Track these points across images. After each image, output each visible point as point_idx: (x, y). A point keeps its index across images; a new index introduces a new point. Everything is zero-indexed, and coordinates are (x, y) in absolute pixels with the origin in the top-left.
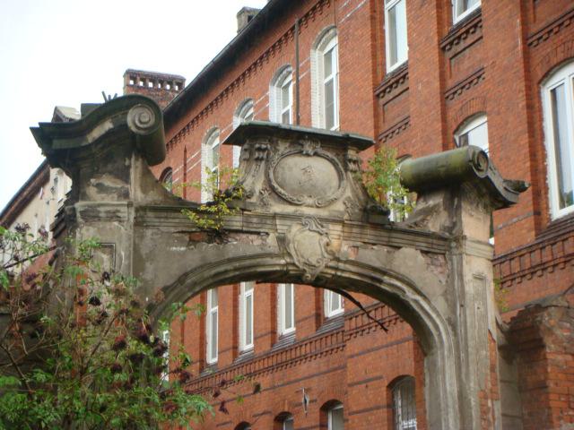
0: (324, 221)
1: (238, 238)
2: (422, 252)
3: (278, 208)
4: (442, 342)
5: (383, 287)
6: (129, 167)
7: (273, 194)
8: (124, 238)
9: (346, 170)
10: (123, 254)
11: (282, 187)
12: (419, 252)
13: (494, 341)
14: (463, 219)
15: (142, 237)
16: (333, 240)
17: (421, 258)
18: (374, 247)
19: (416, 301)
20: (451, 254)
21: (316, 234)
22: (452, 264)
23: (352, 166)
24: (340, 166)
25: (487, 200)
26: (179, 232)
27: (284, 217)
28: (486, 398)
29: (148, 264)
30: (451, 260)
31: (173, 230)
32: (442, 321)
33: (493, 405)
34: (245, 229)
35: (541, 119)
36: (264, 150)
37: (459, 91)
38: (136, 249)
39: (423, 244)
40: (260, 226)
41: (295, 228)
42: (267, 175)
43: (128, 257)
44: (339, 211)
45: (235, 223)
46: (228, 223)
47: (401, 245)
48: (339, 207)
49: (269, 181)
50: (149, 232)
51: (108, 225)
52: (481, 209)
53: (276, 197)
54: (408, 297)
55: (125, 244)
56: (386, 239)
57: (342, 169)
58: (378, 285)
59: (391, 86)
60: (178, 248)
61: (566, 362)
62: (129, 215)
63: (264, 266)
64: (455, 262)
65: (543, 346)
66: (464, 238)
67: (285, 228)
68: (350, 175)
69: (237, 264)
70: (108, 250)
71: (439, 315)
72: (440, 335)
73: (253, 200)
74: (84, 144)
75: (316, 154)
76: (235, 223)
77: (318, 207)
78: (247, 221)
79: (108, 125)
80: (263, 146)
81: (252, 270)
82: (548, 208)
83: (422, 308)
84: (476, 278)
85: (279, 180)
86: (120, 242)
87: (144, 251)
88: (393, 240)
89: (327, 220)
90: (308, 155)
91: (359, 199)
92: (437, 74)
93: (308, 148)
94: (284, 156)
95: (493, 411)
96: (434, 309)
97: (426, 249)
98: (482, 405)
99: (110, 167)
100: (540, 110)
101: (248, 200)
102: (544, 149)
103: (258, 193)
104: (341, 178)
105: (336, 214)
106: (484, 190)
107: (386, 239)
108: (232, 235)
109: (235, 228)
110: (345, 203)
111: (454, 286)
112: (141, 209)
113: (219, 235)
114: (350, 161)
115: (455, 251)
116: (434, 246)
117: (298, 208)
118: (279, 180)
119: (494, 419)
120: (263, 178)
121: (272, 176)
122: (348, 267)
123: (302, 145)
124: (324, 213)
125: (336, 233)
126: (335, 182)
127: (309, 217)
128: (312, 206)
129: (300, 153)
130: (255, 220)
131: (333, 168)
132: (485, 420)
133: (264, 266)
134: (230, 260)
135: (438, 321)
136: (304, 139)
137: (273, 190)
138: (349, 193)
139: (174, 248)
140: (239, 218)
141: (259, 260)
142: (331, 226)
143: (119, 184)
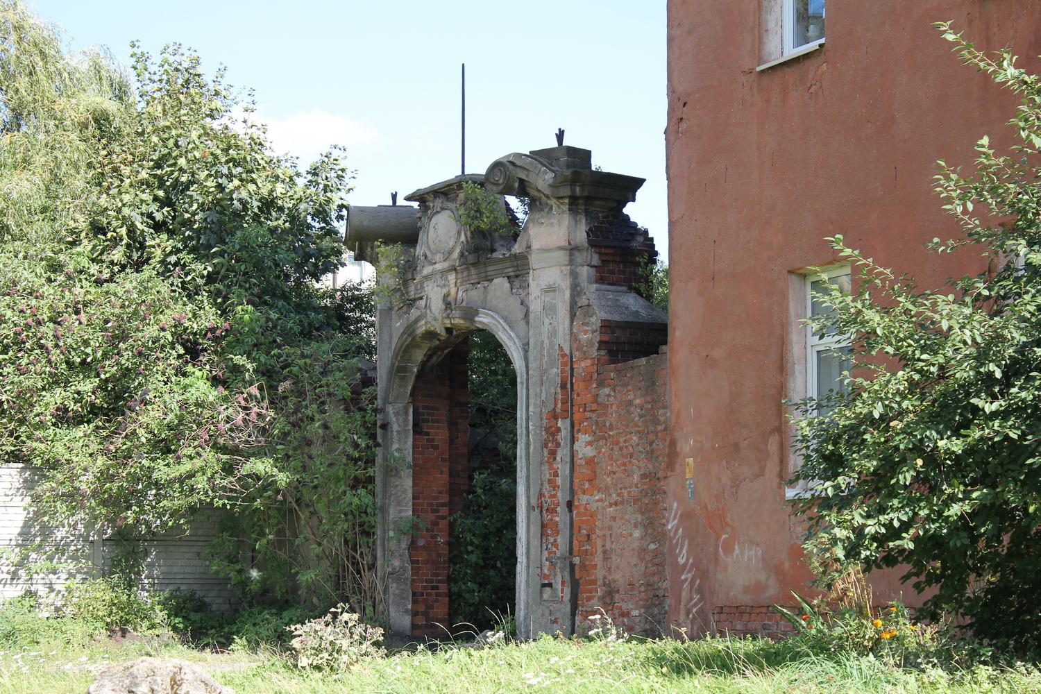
28: (556, 418)
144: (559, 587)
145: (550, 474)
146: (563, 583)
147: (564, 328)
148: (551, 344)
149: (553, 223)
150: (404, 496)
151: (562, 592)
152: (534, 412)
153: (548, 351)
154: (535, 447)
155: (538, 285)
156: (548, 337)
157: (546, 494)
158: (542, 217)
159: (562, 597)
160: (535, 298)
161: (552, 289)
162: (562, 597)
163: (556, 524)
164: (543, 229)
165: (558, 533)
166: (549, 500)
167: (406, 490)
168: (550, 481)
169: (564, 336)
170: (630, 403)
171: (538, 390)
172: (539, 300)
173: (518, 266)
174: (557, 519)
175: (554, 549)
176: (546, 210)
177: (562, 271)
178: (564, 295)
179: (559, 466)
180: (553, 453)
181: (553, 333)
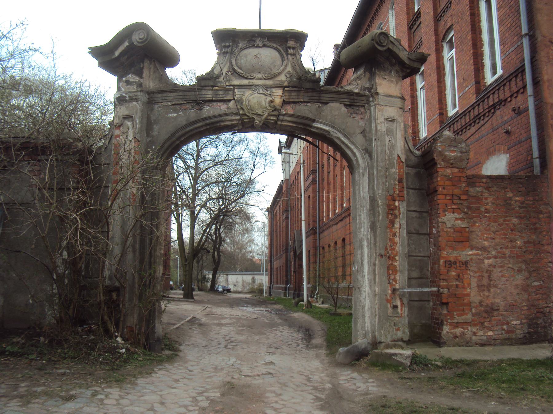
0: (267, 87)
1: (211, 105)
2: (346, 105)
3: (236, 82)
4: (358, 164)
5: (312, 130)
6: (143, 68)
7: (235, 74)
8: (139, 111)
9: (287, 54)
10: (138, 121)
11: (240, 68)
12: (343, 105)
13: (403, 163)
14: (377, 81)
15: (152, 110)
16: (276, 99)
17: (344, 109)
18: (308, 104)
19: (338, 138)
20: (370, 106)
21: (263, 96)
22: (370, 113)
23: (290, 51)
24: (282, 51)
25: (397, 67)
26: (172, 105)
27: (240, 86)
28: (394, 200)
29: (155, 126)
30: (370, 110)
31: (169, 104)
32: (359, 151)
33: (399, 205)
34: (214, 99)
35: (480, 21)
36: (229, 46)
37: (443, 15)
38: (148, 118)
39: (346, 100)
40: (224, 96)
41: (248, 93)
42: (230, 62)
43: (141, 122)
44: (281, 81)
45: (208, 96)
46: (205, 96)
47: (328, 101)
48: (283, 78)
49: (232, 65)
50: (156, 106)
51: (131, 105)
52: (393, 74)
53: (237, 75)
55: (139, 114)
56: (318, 98)
57: (284, 54)
58: (309, 129)
59: (415, 21)
60: (173, 115)
61: (453, 173)
62: (144, 98)
63: (226, 121)
64: (372, 111)
65: (435, 164)
66: (377, 94)
67: (242, 93)
68: (290, 57)
69: (208, 122)
70: (131, 119)
71: (356, 147)
72: (357, 160)
73: (221, 79)
74: (114, 57)
75: (264, 46)
76: (208, 96)
77: (265, 79)
78: (216, 93)
79: (126, 44)
80: (227, 44)
81: (218, 124)
82: (484, 78)
83: (343, 143)
84: (387, 120)
85: (239, 64)
86: (137, 113)
87: (153, 118)
88: (322, 98)
89: (271, 87)
90: (258, 47)
91: (297, 73)
92: (431, 6)
93: (259, 42)
94: (242, 49)
95: (399, 208)
96: (353, 143)
97: (348, 103)
98: (389, 206)
99: (133, 69)
100: (479, 15)
101: (217, 80)
102: (481, 40)
103: (224, 74)
104: (283, 61)
105: (278, 82)
106: (394, 61)
107: (318, 98)
108: (207, 104)
109: (207, 99)
110: (286, 75)
111: (371, 126)
112: (150, 93)
113: (199, 103)
114: (290, 48)
115: (372, 104)
116: (355, 101)
117: (250, 81)
118: (239, 64)
120: (228, 64)
121: (233, 62)
122: (287, 118)
123: (254, 41)
124: (269, 82)
125: (277, 94)
126: (279, 62)
127: (258, 86)
128: (261, 79)
129: (253, 46)
130: (221, 92)
131: (277, 54)
132: (392, 214)
133: (226, 121)
134: (204, 119)
135: (355, 151)
136: (256, 37)
137: (234, 70)
138: (289, 69)
139: (170, 115)
140: (210, 92)
141: (223, 118)
142: (274, 91)
143: (137, 79)
147: (401, 145)
148: (391, 153)
149: (392, 81)
152: (382, 194)
154: (383, 217)
158: (385, 75)
160: (381, 122)
161: (391, 120)
164: (384, 82)
169: (401, 150)
170: (510, 199)
171: (384, 180)
173: (354, 99)
174: (396, 264)
176: (388, 72)
177: (398, 111)
178: (400, 125)
179: (398, 230)
180: (392, 223)
181: (392, 147)
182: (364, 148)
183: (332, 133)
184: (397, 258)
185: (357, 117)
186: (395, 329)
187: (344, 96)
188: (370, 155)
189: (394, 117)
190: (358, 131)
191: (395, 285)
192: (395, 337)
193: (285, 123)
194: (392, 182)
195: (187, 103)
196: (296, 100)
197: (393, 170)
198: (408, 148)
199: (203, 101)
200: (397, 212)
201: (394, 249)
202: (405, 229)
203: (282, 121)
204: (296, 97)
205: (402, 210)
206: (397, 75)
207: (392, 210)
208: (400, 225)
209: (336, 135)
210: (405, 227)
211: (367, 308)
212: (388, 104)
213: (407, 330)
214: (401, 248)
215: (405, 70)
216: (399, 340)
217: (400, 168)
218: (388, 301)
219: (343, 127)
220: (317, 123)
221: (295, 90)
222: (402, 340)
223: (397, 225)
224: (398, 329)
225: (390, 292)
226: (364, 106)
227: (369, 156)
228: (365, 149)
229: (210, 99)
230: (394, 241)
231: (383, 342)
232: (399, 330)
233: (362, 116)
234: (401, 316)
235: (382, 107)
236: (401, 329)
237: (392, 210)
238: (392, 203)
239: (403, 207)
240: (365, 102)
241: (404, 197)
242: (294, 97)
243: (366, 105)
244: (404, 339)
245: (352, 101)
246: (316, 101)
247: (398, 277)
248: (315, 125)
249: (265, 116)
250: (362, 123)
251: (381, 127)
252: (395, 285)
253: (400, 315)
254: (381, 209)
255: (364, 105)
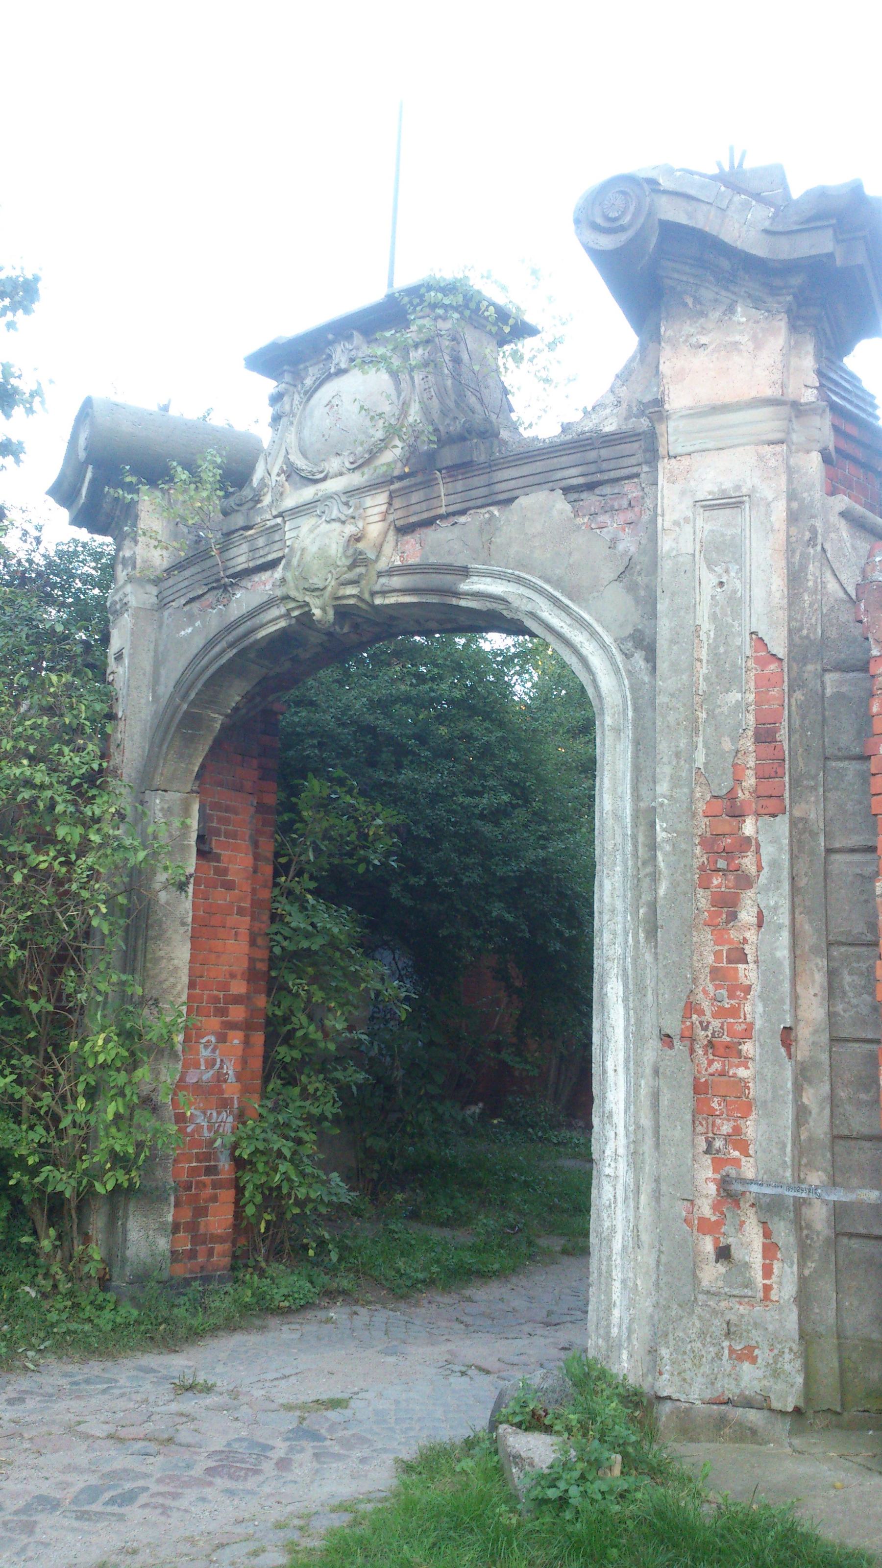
5: (463, 603)
18: (462, 519)
28: (737, 815)
31: (183, 601)
52: (741, 315)
54: (517, 610)
84: (706, 508)
97: (581, 480)
106: (726, 264)
109: (239, 568)
116: (604, 466)
119: (760, 868)
122: (396, 582)
139: (183, 633)
141: (257, 621)
144: (756, 1259)
145: (717, 954)
146: (770, 1250)
147: (769, 593)
148: (723, 633)
150: (172, 980)
151: (767, 1272)
152: (671, 798)
153: (713, 650)
154: (674, 885)
155: (683, 493)
156: (714, 617)
157: (706, 1005)
158: (703, 330)
159: (767, 1289)
160: (677, 523)
162: (767, 1289)
163: (742, 1084)
164: (699, 361)
165: (746, 1109)
166: (716, 1024)
167: (176, 968)
168: (716, 973)
172: (688, 529)
174: (742, 1073)
175: (736, 1154)
177: (761, 458)
178: (768, 514)
179: (751, 935)
182: (629, 630)
183: (516, 602)
184: (747, 1048)
185: (612, 524)
186: (731, 1351)
187: (564, 460)
188: (651, 656)
189: (738, 487)
190: (608, 573)
191: (736, 1162)
192: (731, 1389)
193: (391, 600)
194: (727, 745)
195: (209, 590)
196: (425, 515)
197: (735, 696)
198: (841, 594)
199: (234, 576)
200: (748, 863)
201: (734, 1012)
202: (780, 927)
203: (383, 593)
204: (424, 506)
205: (768, 851)
206: (759, 315)
207: (728, 853)
208: (760, 916)
209: (529, 607)
210: (784, 919)
211: (617, 1245)
212: (710, 445)
213: (792, 1366)
214: (760, 1009)
215: (778, 282)
216: (748, 1403)
217: (763, 684)
218: (704, 1226)
219: (558, 572)
220: (475, 579)
221: (416, 485)
222: (762, 1404)
223: (747, 916)
224: (748, 1355)
225: (712, 1188)
226: (637, 475)
227: (647, 660)
228: (632, 636)
229: (245, 566)
230: (736, 978)
231: (669, 1398)
232: (754, 1360)
233: (630, 516)
234: (766, 1298)
235: (686, 461)
236: (763, 1355)
237: (728, 853)
238: (725, 825)
239: (774, 841)
240: (639, 457)
241: (780, 797)
242: (417, 508)
243: (646, 468)
244: (776, 1405)
245: (593, 468)
246: (479, 502)
247: (751, 1129)
248: (465, 586)
249: (328, 593)
250: (628, 544)
251: (676, 540)
252: (736, 1162)
253: (761, 1295)
254: (666, 855)
255: (635, 470)
